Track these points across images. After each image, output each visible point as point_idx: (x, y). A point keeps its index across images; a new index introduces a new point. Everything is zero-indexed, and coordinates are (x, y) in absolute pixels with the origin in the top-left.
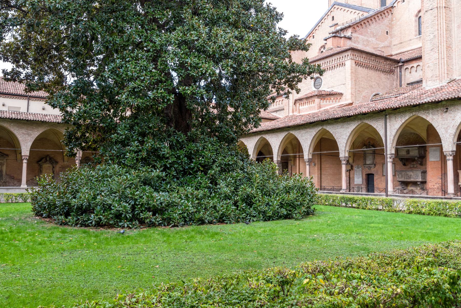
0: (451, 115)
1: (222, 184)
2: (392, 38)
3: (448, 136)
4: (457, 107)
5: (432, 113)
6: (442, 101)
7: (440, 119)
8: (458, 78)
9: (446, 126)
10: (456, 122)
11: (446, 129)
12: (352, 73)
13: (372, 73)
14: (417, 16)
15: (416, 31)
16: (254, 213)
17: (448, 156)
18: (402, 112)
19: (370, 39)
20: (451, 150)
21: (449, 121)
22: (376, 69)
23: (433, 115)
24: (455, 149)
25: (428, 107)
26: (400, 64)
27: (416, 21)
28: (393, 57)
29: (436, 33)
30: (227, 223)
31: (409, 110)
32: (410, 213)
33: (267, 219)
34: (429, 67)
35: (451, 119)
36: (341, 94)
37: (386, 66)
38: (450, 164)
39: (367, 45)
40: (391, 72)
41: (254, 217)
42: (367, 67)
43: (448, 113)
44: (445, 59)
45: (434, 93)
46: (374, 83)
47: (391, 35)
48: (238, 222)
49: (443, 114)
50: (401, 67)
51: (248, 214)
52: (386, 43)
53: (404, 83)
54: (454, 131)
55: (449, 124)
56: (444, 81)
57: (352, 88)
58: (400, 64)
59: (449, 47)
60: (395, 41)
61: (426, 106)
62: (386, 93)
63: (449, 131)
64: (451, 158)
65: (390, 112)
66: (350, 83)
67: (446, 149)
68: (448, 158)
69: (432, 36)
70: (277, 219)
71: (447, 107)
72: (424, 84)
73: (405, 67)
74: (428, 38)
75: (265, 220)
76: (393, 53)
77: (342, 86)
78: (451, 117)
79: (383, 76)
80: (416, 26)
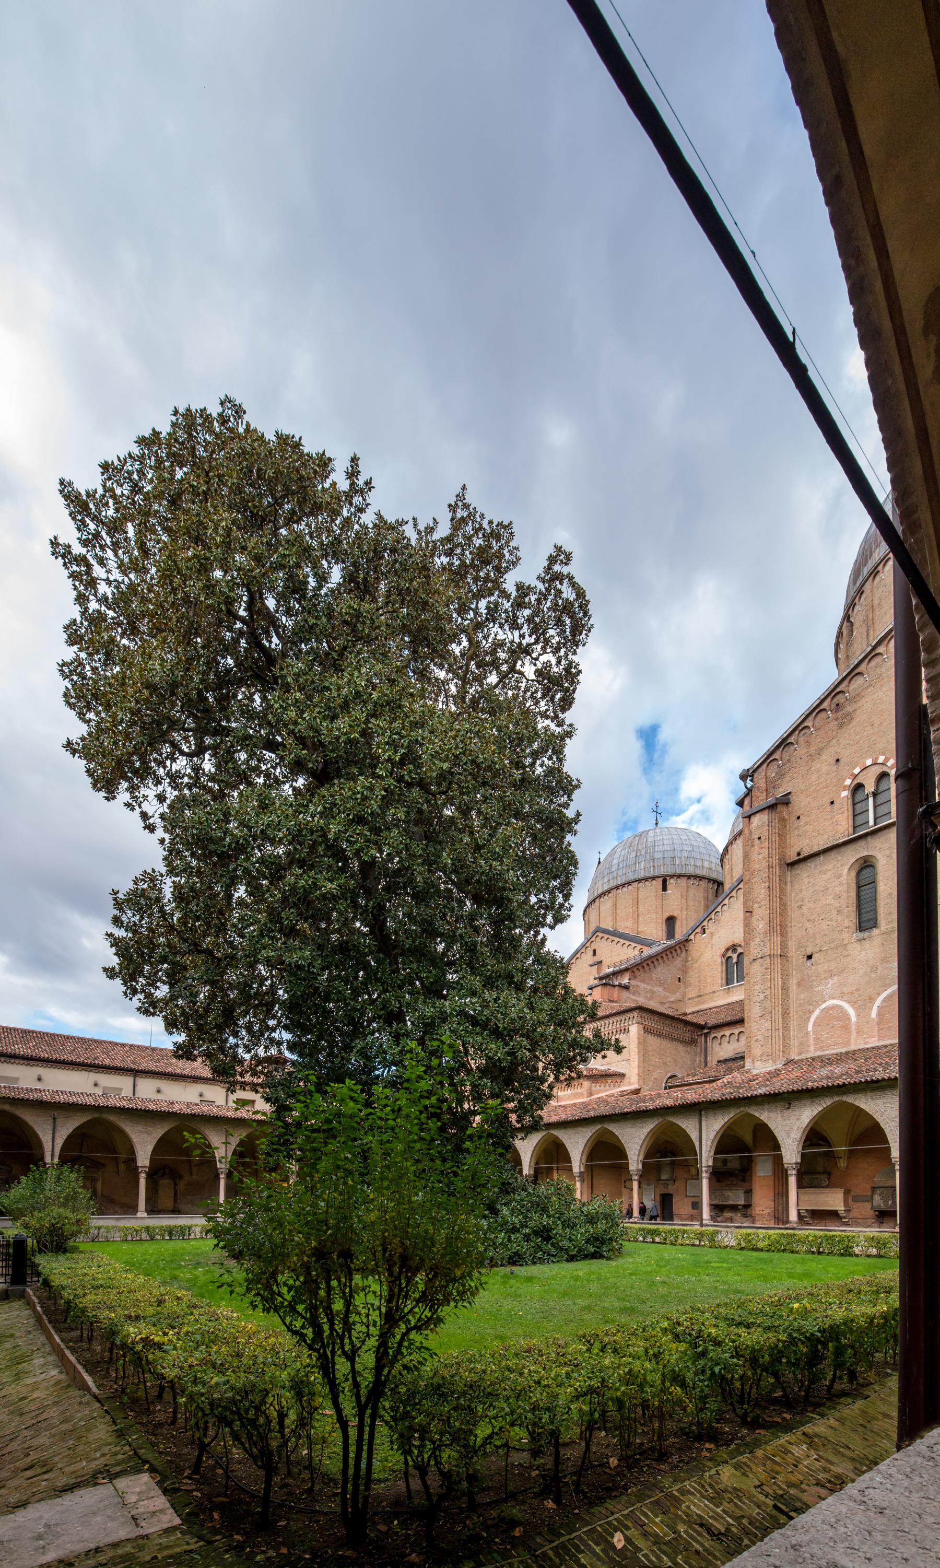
1: (505, 1211)
2: (686, 987)
3: (790, 1141)
4: (803, 1102)
6: (784, 1092)
7: (780, 1118)
8: (797, 1058)
9: (788, 1128)
12: (639, 1043)
13: (666, 1044)
14: (723, 956)
15: (722, 979)
16: (553, 1251)
19: (655, 989)
20: (794, 1161)
22: (672, 1038)
24: (799, 1160)
26: (706, 1031)
27: (722, 963)
28: (689, 1018)
29: (768, 992)
30: (522, 1265)
32: (742, 1249)
33: (571, 1259)
34: (757, 1040)
36: (623, 1075)
37: (686, 1034)
38: (792, 1181)
39: (651, 998)
40: (693, 1042)
41: (553, 1256)
42: (660, 1035)
44: (781, 1031)
45: (768, 1080)
46: (669, 1059)
47: (684, 983)
48: (534, 1263)
50: (706, 1035)
51: (544, 1253)
52: (678, 996)
53: (712, 1060)
54: (800, 1135)
56: (778, 1062)
57: (639, 1067)
58: (706, 1031)
59: (785, 1014)
60: (691, 993)
61: (759, 1099)
62: (688, 1075)
63: (792, 1135)
64: (794, 1172)
66: (636, 1060)
68: (790, 1172)
69: (762, 996)
70: (584, 1259)
72: (748, 1064)
73: (713, 1035)
74: (756, 999)
75: (567, 1261)
76: (688, 1011)
77: (624, 1063)
79: (681, 1048)
80: (722, 971)
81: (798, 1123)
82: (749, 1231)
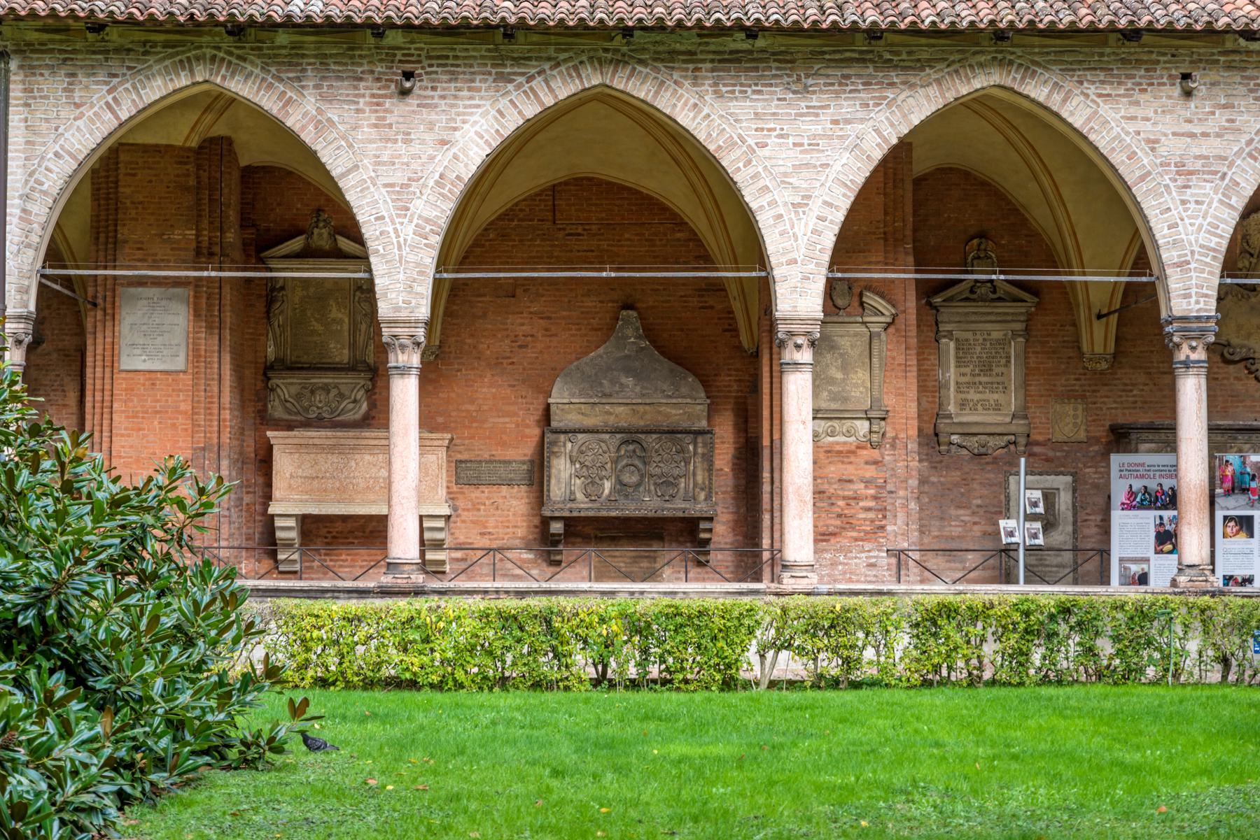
0: (433, 117)
5: (316, 87)
9: (399, 177)
10: (456, 157)
11: (402, 194)
17: (403, 347)
18: (117, 50)
21: (416, 148)
23: (323, 98)
25: (295, 46)
31: (166, 45)
35: (429, 137)
43: (412, 101)
49: (388, 103)
55: (415, 166)
63: (419, 206)
64: (415, 360)
65: (33, 36)
67: (398, 309)
71: (408, 67)
78: (431, 126)
81: (443, 159)
82: (354, 606)
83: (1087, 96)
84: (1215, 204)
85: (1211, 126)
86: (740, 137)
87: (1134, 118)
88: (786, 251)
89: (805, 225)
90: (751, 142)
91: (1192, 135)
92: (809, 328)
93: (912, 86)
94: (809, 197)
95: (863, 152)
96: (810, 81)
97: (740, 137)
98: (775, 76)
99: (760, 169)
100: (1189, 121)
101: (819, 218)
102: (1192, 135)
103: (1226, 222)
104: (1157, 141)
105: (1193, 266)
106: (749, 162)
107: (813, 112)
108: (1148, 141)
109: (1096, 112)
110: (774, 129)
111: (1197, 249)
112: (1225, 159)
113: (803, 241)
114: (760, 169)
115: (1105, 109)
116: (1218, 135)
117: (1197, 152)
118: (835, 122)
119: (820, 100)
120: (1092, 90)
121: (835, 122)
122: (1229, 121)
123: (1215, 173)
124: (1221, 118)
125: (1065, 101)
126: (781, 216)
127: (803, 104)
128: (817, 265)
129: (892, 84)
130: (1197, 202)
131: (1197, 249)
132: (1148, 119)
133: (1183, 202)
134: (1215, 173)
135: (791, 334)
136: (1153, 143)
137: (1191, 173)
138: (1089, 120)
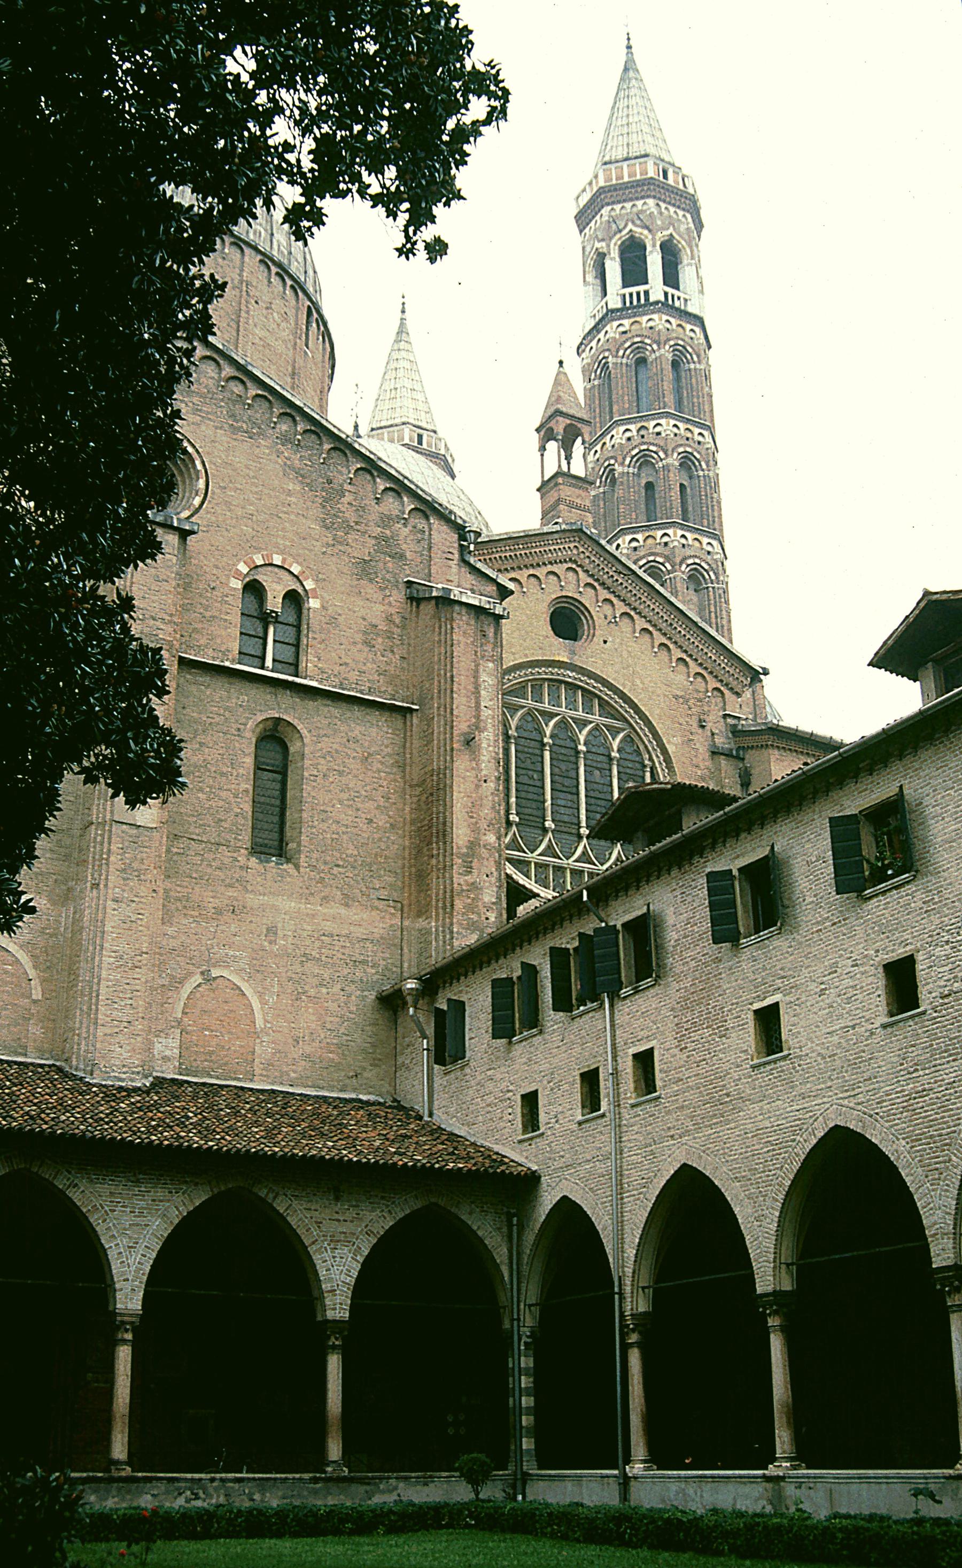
83: (286, 1196)
84: (350, 1259)
85: (348, 1216)
86: (101, 1205)
87: (310, 1209)
88: (123, 1273)
89: (134, 1259)
90: (107, 1208)
91: (338, 1220)
92: (134, 1319)
93: (196, 1184)
94: (137, 1243)
95: (168, 1219)
96: (141, 1176)
97: (101, 1205)
98: (122, 1172)
99: (111, 1225)
100: (337, 1213)
101: (142, 1255)
102: (338, 1220)
103: (355, 1269)
104: (321, 1223)
105: (338, 1292)
106: (104, 1221)
107: (142, 1194)
108: (316, 1222)
109: (291, 1205)
110: (119, 1202)
111: (340, 1283)
112: (354, 1234)
113: (133, 1268)
114: (111, 1225)
115: (295, 1203)
116: (352, 1222)
117: (340, 1229)
118: (153, 1200)
119: (146, 1187)
120: (289, 1193)
121: (153, 1200)
122: (358, 1214)
123: (350, 1242)
124: (352, 1213)
125: (275, 1198)
126: (121, 1253)
127: (136, 1189)
128: (141, 1282)
129: (186, 1182)
130: (342, 1258)
131: (340, 1283)
132: (316, 1210)
133: (334, 1257)
134: (350, 1242)
135: (123, 1323)
136: (319, 1223)
137: (338, 1241)
138: (286, 1210)
